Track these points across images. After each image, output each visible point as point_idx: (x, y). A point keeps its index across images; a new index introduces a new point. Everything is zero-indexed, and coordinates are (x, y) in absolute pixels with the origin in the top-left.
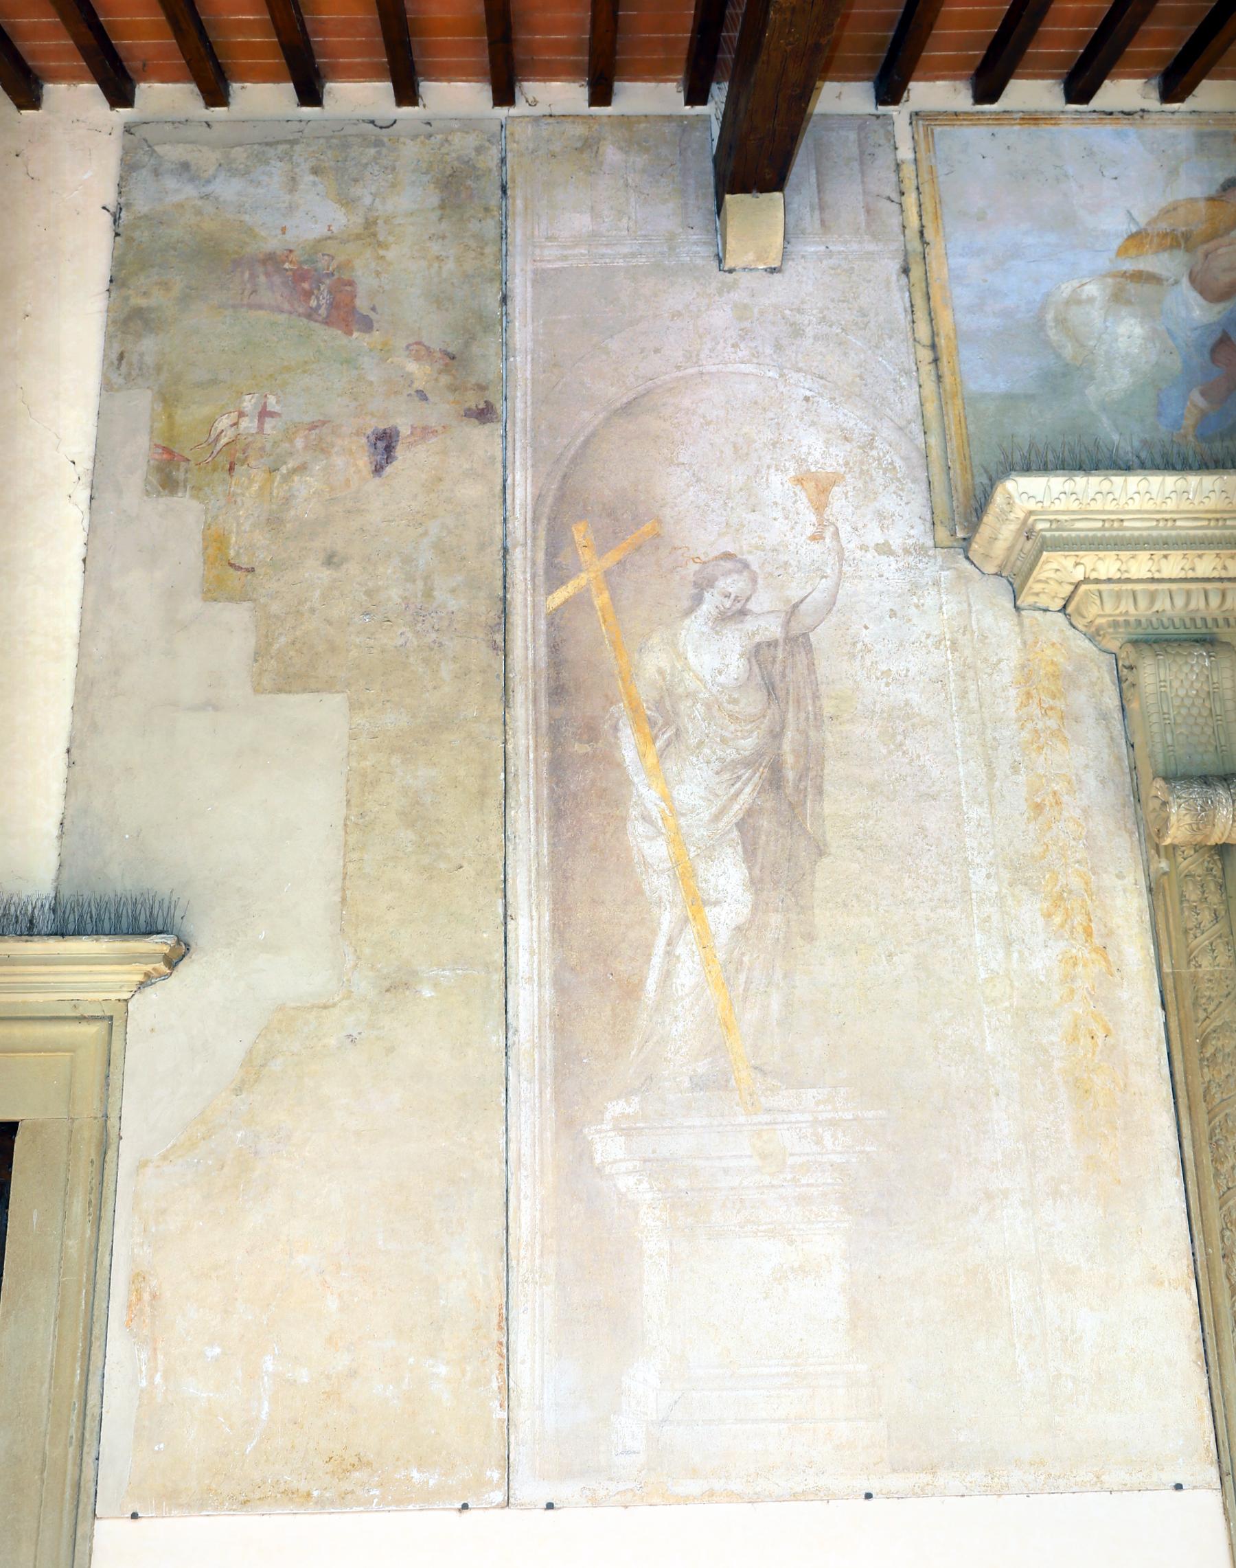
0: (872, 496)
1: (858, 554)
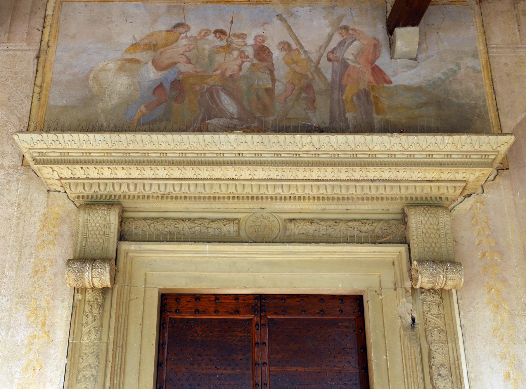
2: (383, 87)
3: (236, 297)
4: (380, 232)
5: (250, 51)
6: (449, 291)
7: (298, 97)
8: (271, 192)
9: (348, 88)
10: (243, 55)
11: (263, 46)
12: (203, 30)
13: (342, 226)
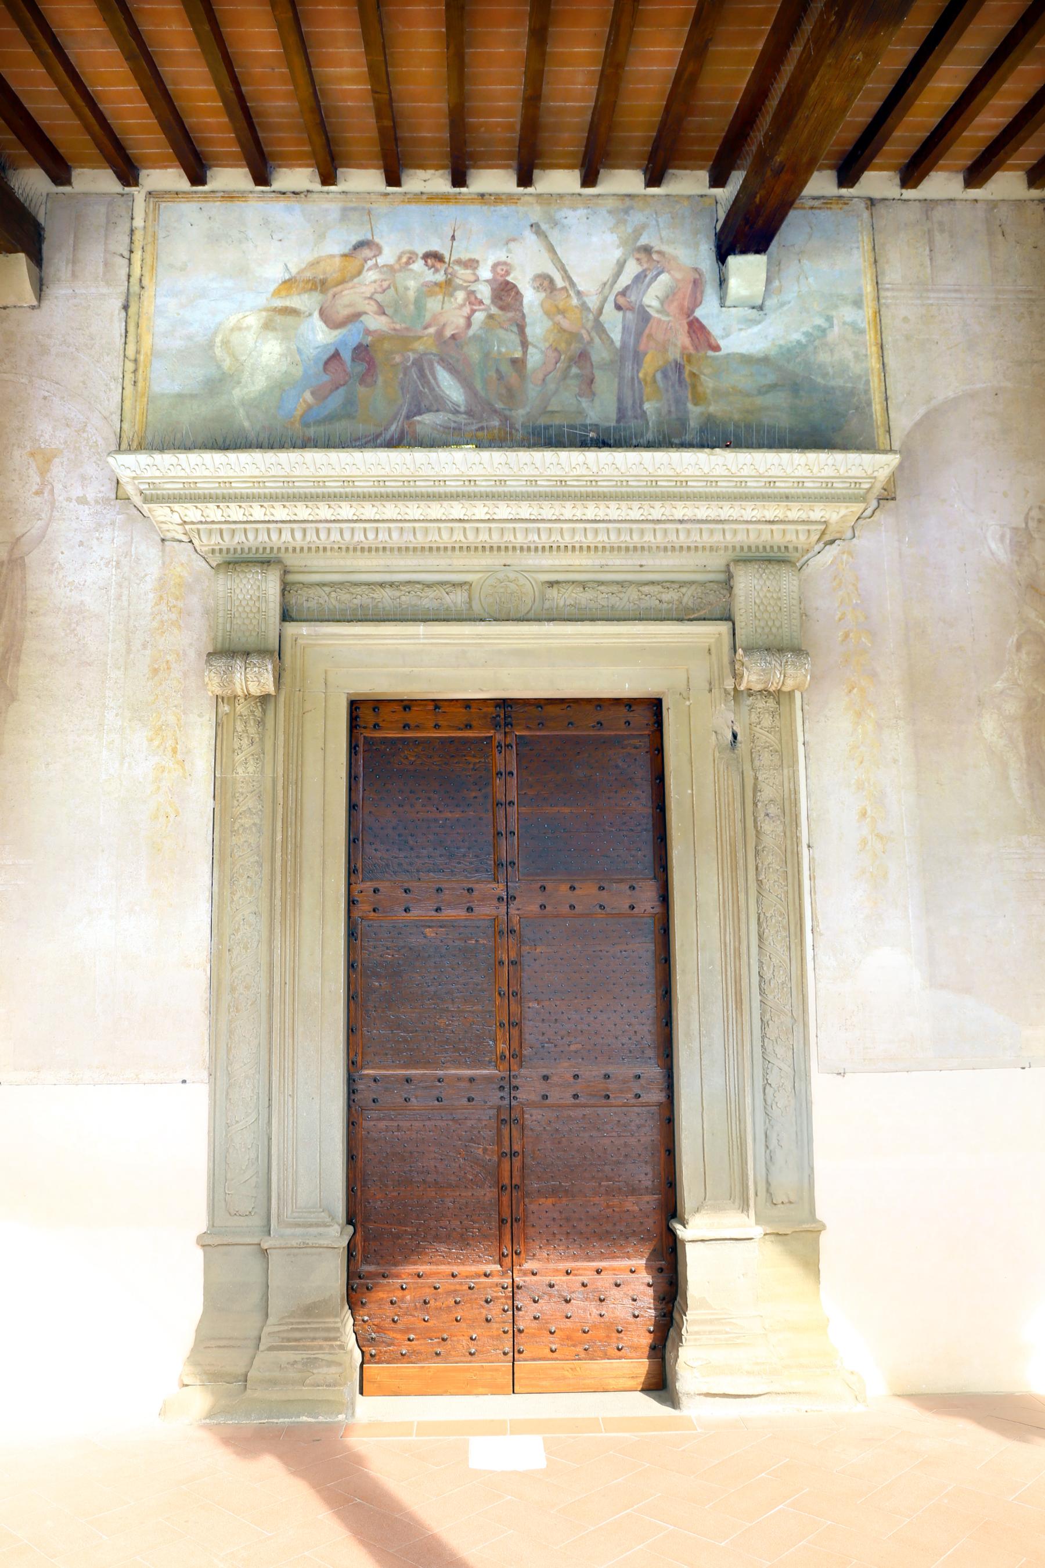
1: (65, 504)
2: (707, 357)
3: (467, 704)
4: (690, 604)
5: (485, 292)
6: (791, 694)
7: (565, 376)
8: (520, 539)
9: (648, 358)
10: (473, 299)
11: (507, 283)
12: (403, 253)
13: (633, 593)
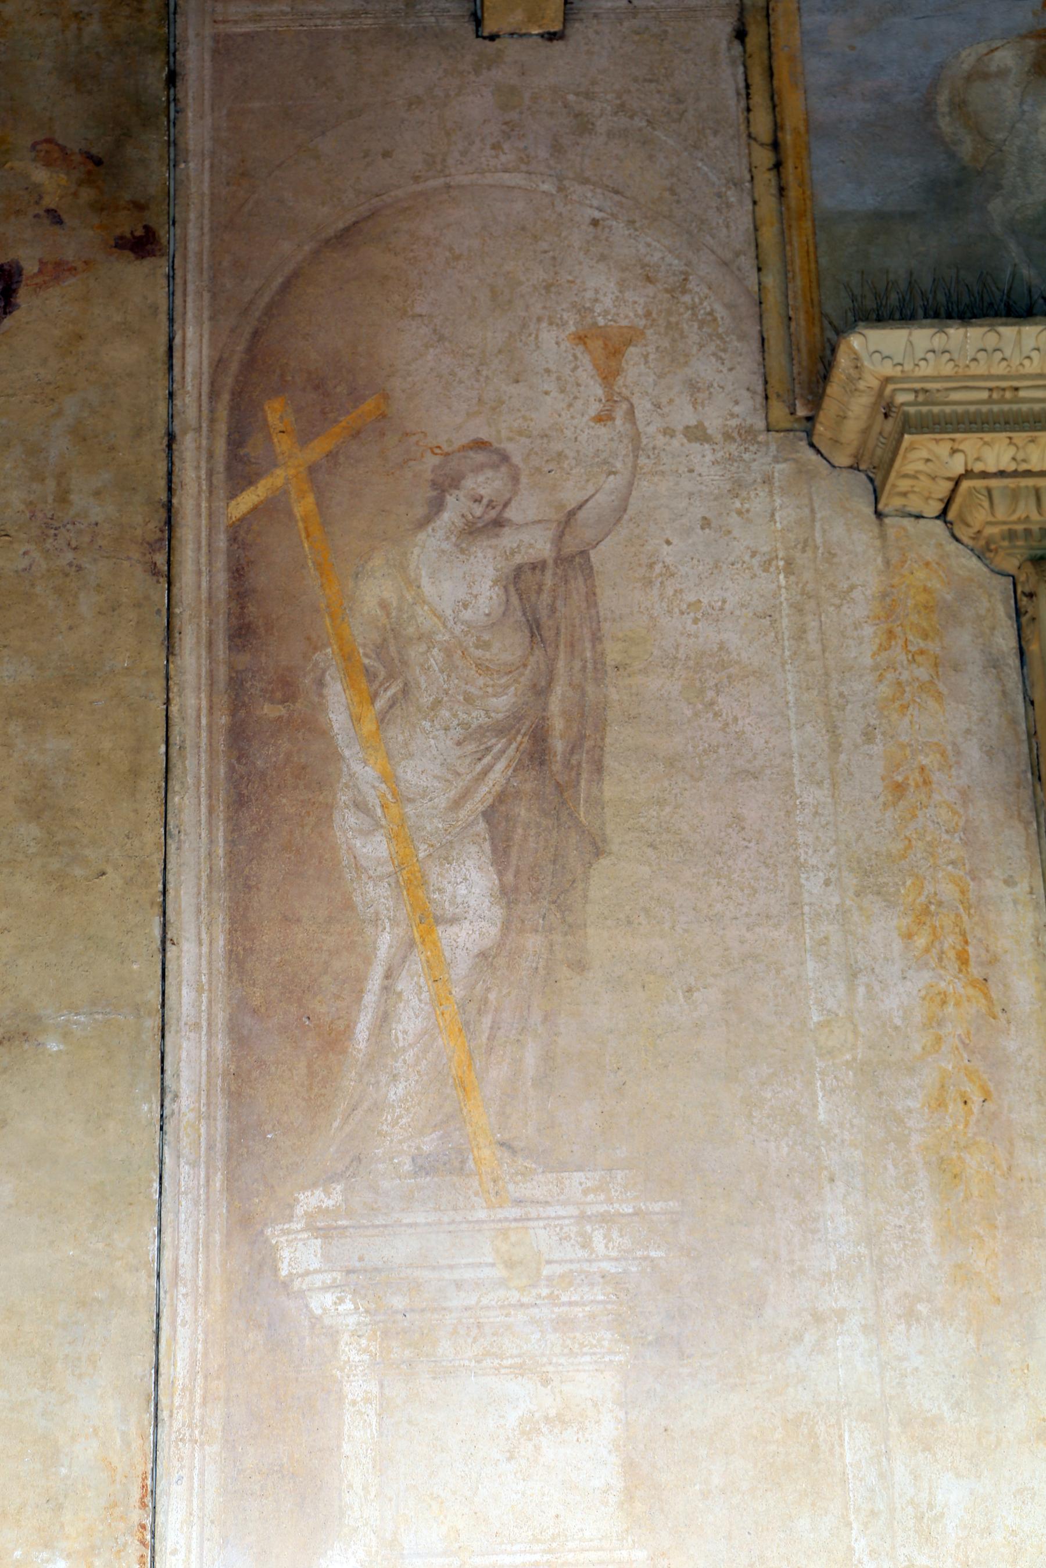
0: (682, 360)
1: (661, 440)
